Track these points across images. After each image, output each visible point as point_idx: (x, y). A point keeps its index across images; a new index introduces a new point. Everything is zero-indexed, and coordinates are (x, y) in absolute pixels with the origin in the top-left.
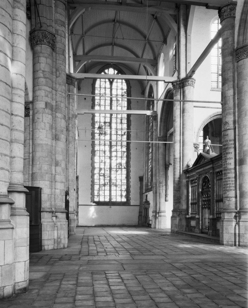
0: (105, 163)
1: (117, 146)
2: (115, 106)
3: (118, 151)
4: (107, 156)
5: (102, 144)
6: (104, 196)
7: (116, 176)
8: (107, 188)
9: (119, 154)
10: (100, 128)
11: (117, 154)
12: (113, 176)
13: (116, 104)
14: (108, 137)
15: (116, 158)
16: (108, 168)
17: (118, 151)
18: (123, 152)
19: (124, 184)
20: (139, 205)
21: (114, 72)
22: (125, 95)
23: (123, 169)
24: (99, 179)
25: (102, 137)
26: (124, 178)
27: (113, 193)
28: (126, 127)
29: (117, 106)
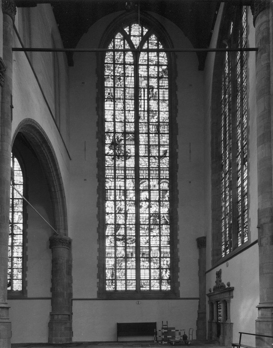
0: (126, 214)
1: (151, 180)
2: (144, 100)
3: (151, 188)
4: (130, 201)
5: (119, 177)
6: (126, 280)
7: (150, 239)
8: (131, 263)
9: (155, 196)
10: (114, 144)
11: (150, 195)
12: (143, 240)
13: (146, 95)
14: (131, 163)
15: (147, 203)
16: (132, 224)
17: (151, 188)
18: (163, 190)
19: (165, 255)
20: (198, 296)
21: (142, 31)
22: (164, 76)
23: (162, 224)
24: (116, 246)
25: (120, 163)
26: (166, 243)
27: (144, 274)
28: (168, 141)
29: (149, 100)
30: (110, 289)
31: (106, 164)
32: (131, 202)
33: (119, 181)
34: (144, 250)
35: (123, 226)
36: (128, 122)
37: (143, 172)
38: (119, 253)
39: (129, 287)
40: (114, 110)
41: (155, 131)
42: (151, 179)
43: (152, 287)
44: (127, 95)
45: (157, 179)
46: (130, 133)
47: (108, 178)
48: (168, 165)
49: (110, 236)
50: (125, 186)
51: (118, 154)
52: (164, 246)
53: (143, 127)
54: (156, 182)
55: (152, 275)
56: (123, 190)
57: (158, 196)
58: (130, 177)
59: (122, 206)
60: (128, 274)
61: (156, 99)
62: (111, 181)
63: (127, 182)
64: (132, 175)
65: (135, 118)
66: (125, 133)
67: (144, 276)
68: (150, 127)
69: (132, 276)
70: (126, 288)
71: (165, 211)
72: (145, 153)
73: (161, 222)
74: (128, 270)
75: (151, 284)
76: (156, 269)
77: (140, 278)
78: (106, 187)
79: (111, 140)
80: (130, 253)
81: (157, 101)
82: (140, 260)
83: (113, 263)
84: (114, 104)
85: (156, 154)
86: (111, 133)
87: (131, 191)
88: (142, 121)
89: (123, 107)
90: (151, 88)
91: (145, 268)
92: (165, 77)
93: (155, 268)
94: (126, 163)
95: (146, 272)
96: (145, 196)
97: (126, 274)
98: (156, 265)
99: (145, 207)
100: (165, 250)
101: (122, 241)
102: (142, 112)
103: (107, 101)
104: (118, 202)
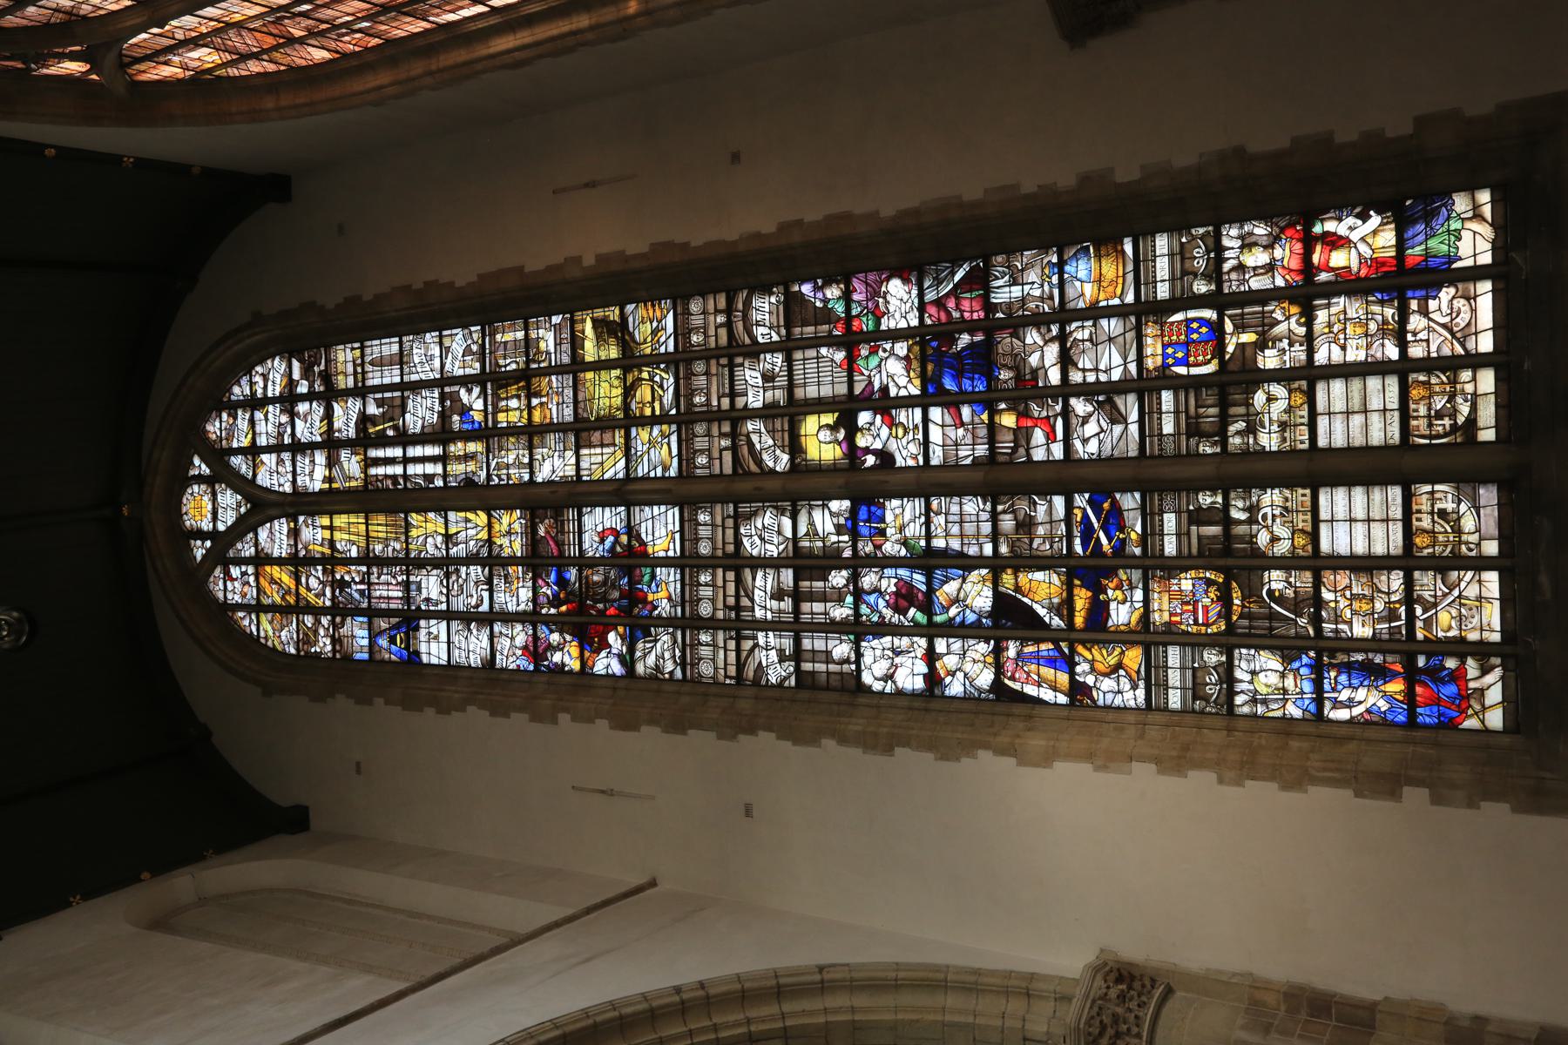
1: (740, 402)
3: (780, 395)
5: (731, 601)
7: (1086, 391)
11: (819, 405)
17: (780, 395)
18: (788, 326)
19: (1200, 264)
21: (200, 479)
22: (322, 367)
24: (1148, 636)
25: (664, 590)
26: (1109, 269)
28: (556, 319)
29: (404, 439)
30: (1494, 695)
31: (671, 673)
32: (864, 529)
33: (752, 600)
34: (1168, 428)
35: (1008, 579)
36: (490, 541)
37: (702, 451)
38: (1195, 612)
39: (1474, 538)
40: (448, 616)
41: (518, 397)
42: (732, 403)
43: (1471, 345)
44: (394, 549)
45: (732, 367)
46: (531, 530)
47: (740, 666)
48: (660, 304)
49: (1072, 674)
50: (774, 564)
51: (625, 602)
52: (1130, 277)
53: (505, 460)
54: (748, 372)
55: (1361, 356)
56: (796, 579)
57: (824, 351)
58: (730, 533)
59: (884, 583)
60: (1360, 548)
61: (398, 402)
62: (752, 650)
63: (755, 553)
64: (719, 521)
65: (473, 510)
66: (535, 561)
67: (1375, 419)
68: (505, 425)
69: (1377, 513)
70: (1480, 564)
71: (906, 297)
72: (614, 445)
73: (975, 316)
74: (1325, 546)
75: (1446, 351)
76: (1309, 324)
77: (1386, 448)
78: (786, 684)
79: (565, 641)
80: (1194, 528)
81: (406, 394)
82: (1246, 453)
83: (1269, 662)
84: (429, 615)
85: (616, 383)
86: (535, 638)
87: (802, 530)
89: (434, 572)
90: (365, 430)
91: (1305, 413)
92: (326, 365)
93: (1302, 331)
94: (662, 554)
95: (1339, 405)
96: (825, 435)
97: (1365, 565)
99: (885, 431)
100: (1162, 268)
101: (1110, 592)
102: (449, 468)
103: (417, 653)
104: (864, 609)
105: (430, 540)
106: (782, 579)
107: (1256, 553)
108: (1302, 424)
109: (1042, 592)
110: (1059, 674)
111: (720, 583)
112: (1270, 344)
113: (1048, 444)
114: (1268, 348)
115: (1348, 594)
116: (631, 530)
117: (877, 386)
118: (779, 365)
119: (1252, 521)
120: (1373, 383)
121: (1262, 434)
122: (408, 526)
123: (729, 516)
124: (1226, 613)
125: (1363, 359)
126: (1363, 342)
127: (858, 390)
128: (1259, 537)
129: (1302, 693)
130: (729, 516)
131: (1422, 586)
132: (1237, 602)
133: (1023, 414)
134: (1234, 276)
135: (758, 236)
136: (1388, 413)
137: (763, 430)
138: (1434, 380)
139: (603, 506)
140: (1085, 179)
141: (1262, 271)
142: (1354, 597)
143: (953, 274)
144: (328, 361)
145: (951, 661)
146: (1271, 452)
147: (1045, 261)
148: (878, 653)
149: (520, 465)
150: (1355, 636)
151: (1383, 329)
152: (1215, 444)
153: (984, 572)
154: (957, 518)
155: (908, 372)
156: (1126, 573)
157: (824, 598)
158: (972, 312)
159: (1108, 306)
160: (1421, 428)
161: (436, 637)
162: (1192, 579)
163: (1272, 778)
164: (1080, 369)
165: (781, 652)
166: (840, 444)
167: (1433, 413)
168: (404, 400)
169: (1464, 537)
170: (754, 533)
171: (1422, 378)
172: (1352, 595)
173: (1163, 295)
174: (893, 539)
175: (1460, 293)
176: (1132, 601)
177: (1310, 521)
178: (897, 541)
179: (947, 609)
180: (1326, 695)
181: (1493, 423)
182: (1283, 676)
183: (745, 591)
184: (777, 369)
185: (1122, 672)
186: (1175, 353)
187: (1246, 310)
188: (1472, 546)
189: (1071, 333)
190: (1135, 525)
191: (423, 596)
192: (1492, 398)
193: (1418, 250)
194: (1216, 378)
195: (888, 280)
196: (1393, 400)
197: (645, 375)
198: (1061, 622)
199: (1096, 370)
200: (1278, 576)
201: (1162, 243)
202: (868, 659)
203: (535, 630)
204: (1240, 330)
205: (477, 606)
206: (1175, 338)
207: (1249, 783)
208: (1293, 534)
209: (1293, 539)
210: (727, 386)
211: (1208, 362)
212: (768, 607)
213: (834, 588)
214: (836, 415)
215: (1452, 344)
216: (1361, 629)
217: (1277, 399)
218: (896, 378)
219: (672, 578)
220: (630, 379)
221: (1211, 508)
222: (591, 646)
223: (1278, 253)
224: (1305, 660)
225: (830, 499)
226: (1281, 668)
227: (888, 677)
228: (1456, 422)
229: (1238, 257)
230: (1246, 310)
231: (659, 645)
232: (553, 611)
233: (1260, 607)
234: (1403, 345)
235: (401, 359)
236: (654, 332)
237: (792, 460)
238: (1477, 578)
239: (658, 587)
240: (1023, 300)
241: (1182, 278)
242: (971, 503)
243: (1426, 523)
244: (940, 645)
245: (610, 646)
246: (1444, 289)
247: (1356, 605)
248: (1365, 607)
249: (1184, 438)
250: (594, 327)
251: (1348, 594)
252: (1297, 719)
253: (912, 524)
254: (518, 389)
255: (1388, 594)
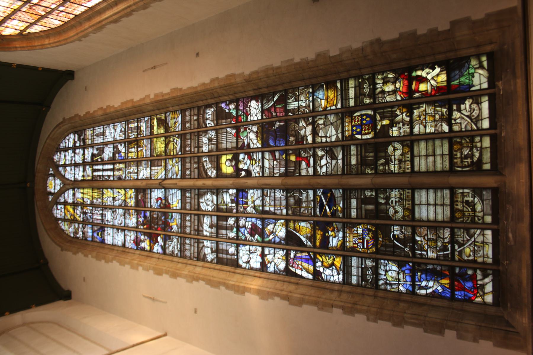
5: (196, 227)
11: (227, 150)
18: (217, 120)
19: (367, 91)
25: (175, 223)
26: (331, 94)
29: (103, 162)
31: (177, 254)
33: (203, 228)
34: (354, 162)
35: (291, 225)
37: (188, 169)
39: (480, 214)
40: (113, 227)
41: (134, 147)
43: (479, 125)
46: (136, 197)
47: (199, 253)
49: (315, 266)
52: (339, 97)
53: (130, 171)
55: (433, 130)
58: (196, 201)
61: (102, 149)
62: (202, 248)
67: (438, 158)
69: (439, 202)
70: (484, 227)
71: (257, 107)
74: (417, 215)
75: (469, 128)
76: (411, 115)
80: (363, 206)
85: (163, 142)
86: (137, 237)
87: (220, 201)
88: (123, 173)
91: (409, 156)
92: (84, 136)
93: (408, 119)
94: (175, 208)
95: (423, 153)
96: (228, 163)
98: (399, 118)
99: (248, 162)
100: (352, 92)
101: (330, 232)
103: (104, 240)
104: (240, 235)
105: (108, 199)
106: (213, 220)
107: (389, 218)
108: (408, 161)
109: (304, 231)
110: (310, 266)
111: (193, 220)
112: (395, 125)
113: (307, 168)
114: (394, 127)
115: (426, 238)
116: (166, 198)
117: (246, 143)
118: (214, 135)
119: (387, 203)
120: (438, 143)
121: (391, 165)
122: (103, 193)
123: (196, 195)
124: (375, 245)
125: (433, 131)
126: (433, 124)
127: (240, 144)
128: (390, 211)
129: (406, 281)
130: (196, 195)
131: (458, 236)
132: (380, 239)
133: (298, 156)
134: (380, 95)
135: (204, 84)
136: (444, 157)
137: (208, 161)
138: (463, 141)
139: (158, 189)
140: (318, 55)
141: (391, 93)
142: (429, 240)
143: (274, 97)
144: (85, 135)
145: (269, 258)
146: (395, 173)
147: (307, 91)
148: (244, 252)
149: (135, 173)
150: (429, 257)
151: (442, 118)
152: (372, 169)
153: (283, 221)
154: (273, 198)
155: (257, 138)
156: (336, 225)
157: (226, 228)
158: (280, 113)
159: (331, 110)
160: (458, 163)
161: (109, 234)
162: (362, 228)
163: (389, 320)
164: (320, 136)
165: (212, 249)
166: (233, 167)
167: (463, 156)
168: (103, 148)
169: (477, 214)
170: (204, 201)
171: (458, 140)
172: (428, 238)
173: (352, 104)
174: (250, 206)
175: (474, 102)
176: (338, 237)
177: (411, 204)
178: (252, 207)
179: (269, 236)
180: (417, 283)
181: (489, 161)
182: (398, 273)
183: (201, 224)
184: (213, 137)
185: (334, 267)
186: (356, 129)
187: (385, 110)
188: (480, 218)
189: (317, 121)
190: (340, 204)
191: (106, 219)
192: (489, 150)
193: (456, 82)
194: (372, 140)
195: (251, 101)
196: (446, 151)
197: (172, 139)
198: (311, 244)
199: (326, 137)
200: (397, 229)
201: (352, 82)
202: (241, 254)
203: (137, 234)
204: (383, 119)
205: (121, 224)
206: (356, 123)
207: (379, 321)
208: (404, 210)
209: (404, 212)
210: (197, 143)
211: (370, 133)
212: (208, 231)
213: (230, 225)
214: (232, 155)
215: (471, 125)
216: (431, 254)
217: (397, 150)
218: (253, 140)
219: (178, 218)
220: (167, 141)
221: (370, 197)
222: (153, 241)
223: (398, 85)
224: (408, 267)
225: (229, 189)
226: (398, 270)
227: (248, 262)
228: (473, 161)
229: (382, 87)
230: (385, 110)
231: (173, 243)
232: (142, 227)
233: (390, 242)
234: (450, 125)
235: (103, 134)
236: (175, 123)
237: (217, 173)
238: (482, 233)
239: (173, 220)
240: (299, 107)
241: (359, 97)
242: (278, 192)
243: (460, 207)
244: (267, 251)
245: (158, 242)
246: (468, 100)
247: (429, 243)
248: (433, 244)
249: (360, 166)
250: (157, 122)
251: (426, 238)
252: (403, 293)
253: (257, 200)
254: (134, 145)
255: (443, 239)
